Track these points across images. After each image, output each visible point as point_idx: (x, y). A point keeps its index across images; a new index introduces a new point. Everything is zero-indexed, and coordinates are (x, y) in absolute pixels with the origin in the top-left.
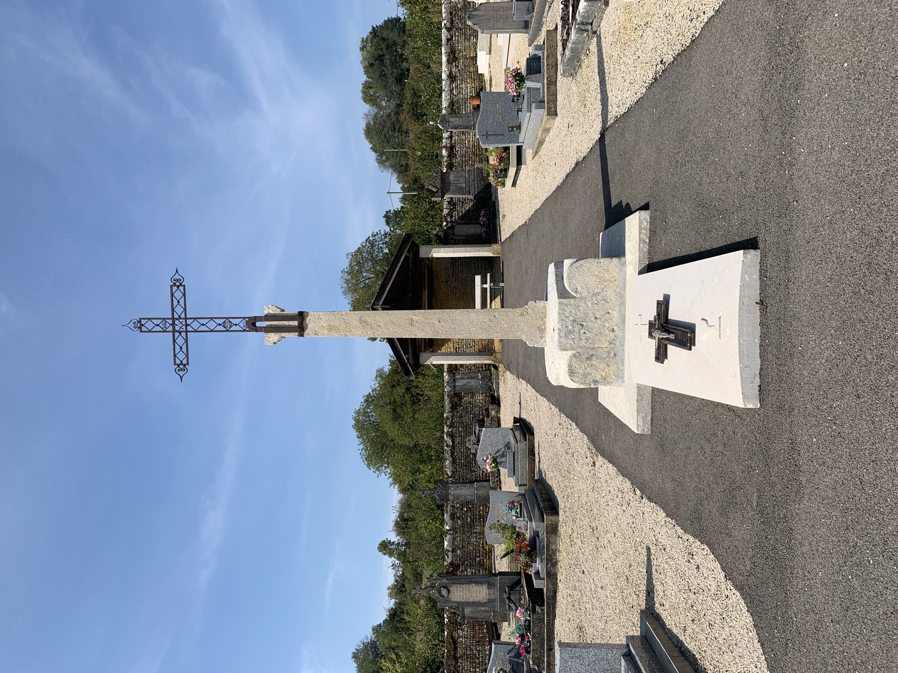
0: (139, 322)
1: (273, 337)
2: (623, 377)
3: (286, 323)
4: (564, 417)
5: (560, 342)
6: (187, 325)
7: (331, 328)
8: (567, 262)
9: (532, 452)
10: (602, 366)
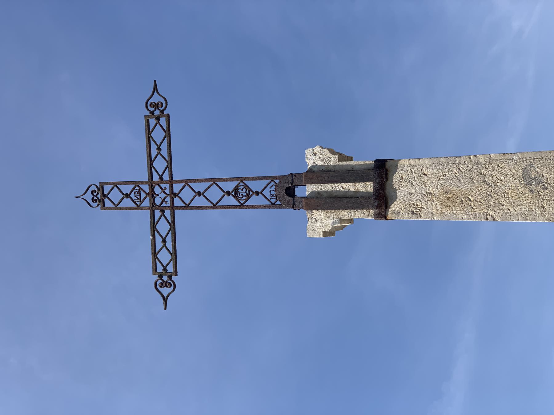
0: (101, 188)
1: (321, 222)
3: (349, 187)
6: (174, 195)
7: (449, 199)
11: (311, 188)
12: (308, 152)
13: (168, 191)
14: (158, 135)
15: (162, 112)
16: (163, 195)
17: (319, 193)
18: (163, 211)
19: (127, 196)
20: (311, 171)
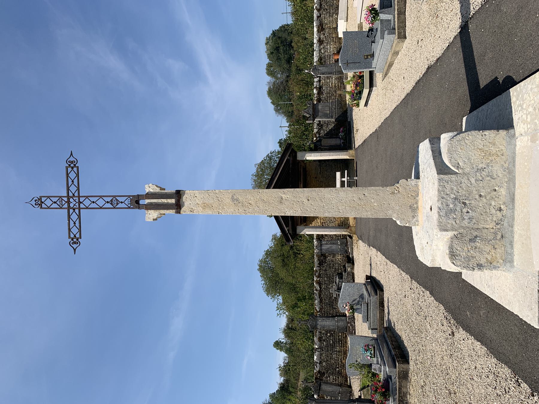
0: (40, 199)
1: (152, 214)
2: (511, 261)
3: (165, 201)
4: (415, 284)
5: (440, 222)
6: (80, 203)
7: (205, 206)
8: (445, 138)
9: (382, 304)
10: (488, 248)
11: (147, 201)
12: (146, 186)
13: (77, 201)
14: (72, 175)
15: (75, 165)
16: (74, 203)
17: (151, 203)
18: (74, 210)
19: (55, 202)
20: (147, 194)
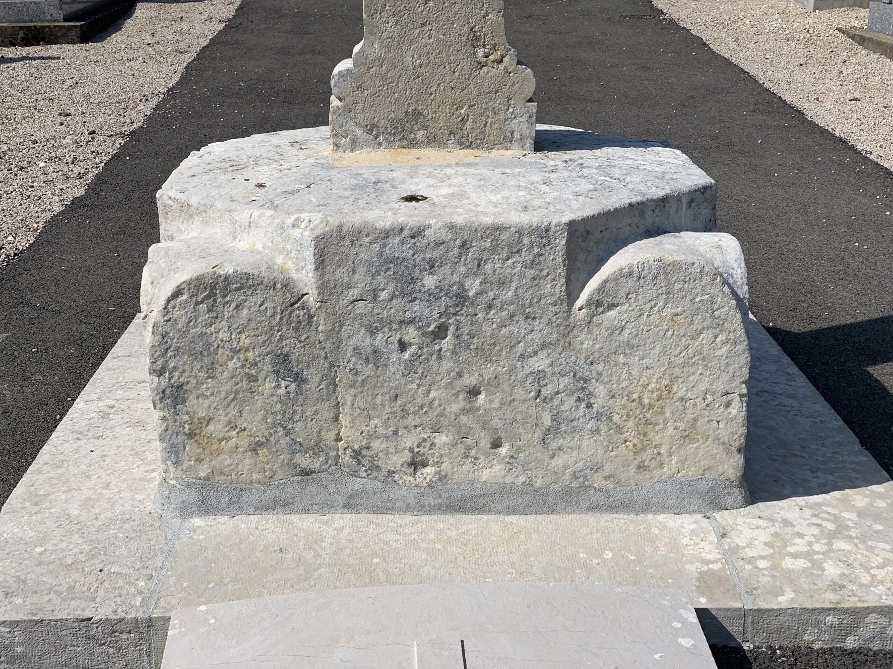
2: (206, 507)
4: (110, 147)
5: (357, 234)
8: (723, 250)
9: (35, 36)
10: (254, 422)
